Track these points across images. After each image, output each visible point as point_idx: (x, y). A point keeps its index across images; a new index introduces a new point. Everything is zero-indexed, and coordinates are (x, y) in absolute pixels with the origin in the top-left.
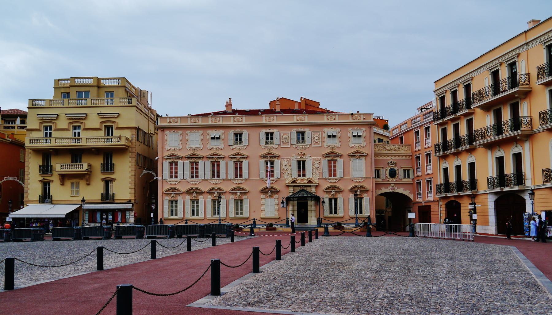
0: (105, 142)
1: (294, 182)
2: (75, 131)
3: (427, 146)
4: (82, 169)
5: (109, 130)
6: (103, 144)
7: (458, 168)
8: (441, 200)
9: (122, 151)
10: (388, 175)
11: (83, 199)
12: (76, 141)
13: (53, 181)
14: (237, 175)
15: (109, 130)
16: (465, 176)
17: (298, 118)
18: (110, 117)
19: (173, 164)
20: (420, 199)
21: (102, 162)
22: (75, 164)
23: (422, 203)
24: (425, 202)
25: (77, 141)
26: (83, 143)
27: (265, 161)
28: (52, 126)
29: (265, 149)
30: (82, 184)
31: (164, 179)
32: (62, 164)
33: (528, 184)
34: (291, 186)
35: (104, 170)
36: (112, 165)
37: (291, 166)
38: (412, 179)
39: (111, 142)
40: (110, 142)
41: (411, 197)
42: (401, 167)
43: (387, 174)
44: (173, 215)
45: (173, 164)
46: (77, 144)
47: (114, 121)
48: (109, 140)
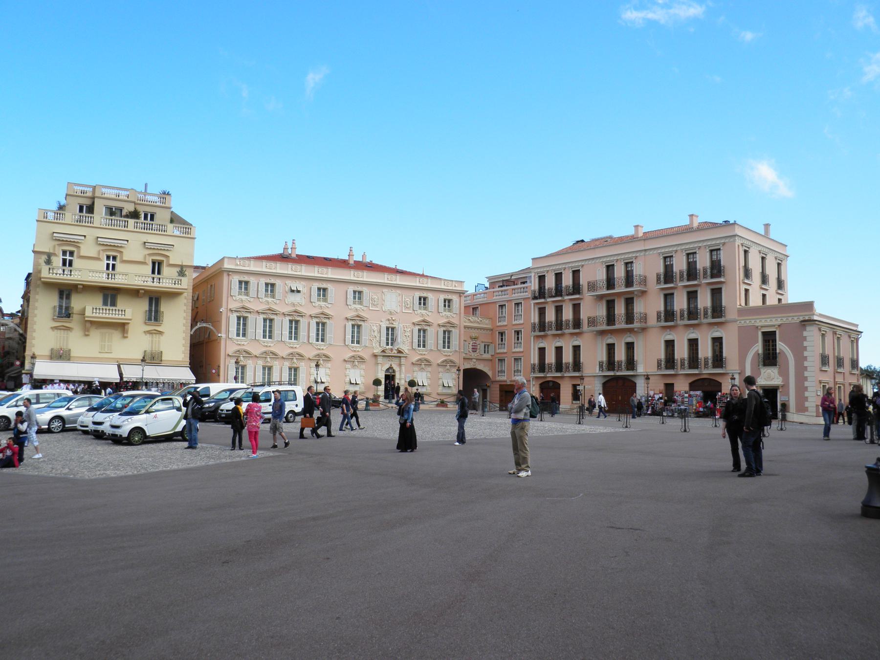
0: (172, 284)
1: (383, 351)
2: (108, 262)
3: (516, 322)
4: (123, 316)
5: (157, 267)
6: (170, 286)
7: (559, 350)
8: (534, 380)
9: (173, 295)
10: (470, 350)
11: (34, 354)
12: (108, 276)
14: (266, 335)
15: (157, 267)
16: (568, 357)
17: (389, 277)
18: (161, 249)
19: (242, 321)
20: (503, 378)
21: (147, 308)
22: (111, 308)
23: (506, 381)
24: (511, 381)
25: (110, 276)
26: (119, 280)
27: (237, 316)
28: (74, 251)
29: (354, 308)
30: (116, 335)
31: (230, 337)
32: (94, 307)
33: (641, 369)
34: (380, 356)
35: (150, 319)
37: (380, 333)
38: (492, 355)
41: (490, 374)
42: (482, 342)
43: (469, 348)
45: (242, 321)
46: (156, 284)
47: (167, 255)
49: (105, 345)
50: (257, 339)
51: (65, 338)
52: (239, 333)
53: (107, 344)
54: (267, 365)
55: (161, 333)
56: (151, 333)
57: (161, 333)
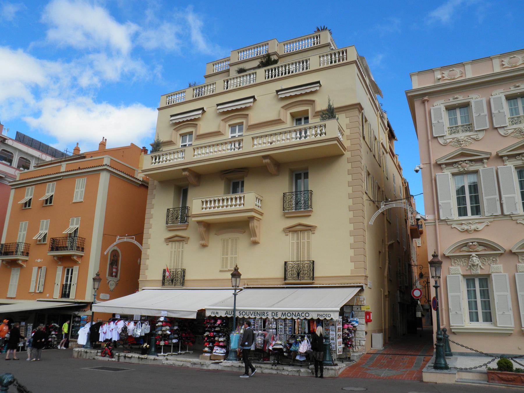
13: (189, 238)
31: (442, 218)
36: (309, 193)
39: (306, 137)
40: (303, 138)
44: (477, 320)
48: (300, 134)
49: (227, 258)
50: (506, 213)
51: (173, 252)
52: (465, 208)
53: (229, 256)
54: (474, 272)
55: (310, 229)
56: (296, 231)
57: (310, 229)
